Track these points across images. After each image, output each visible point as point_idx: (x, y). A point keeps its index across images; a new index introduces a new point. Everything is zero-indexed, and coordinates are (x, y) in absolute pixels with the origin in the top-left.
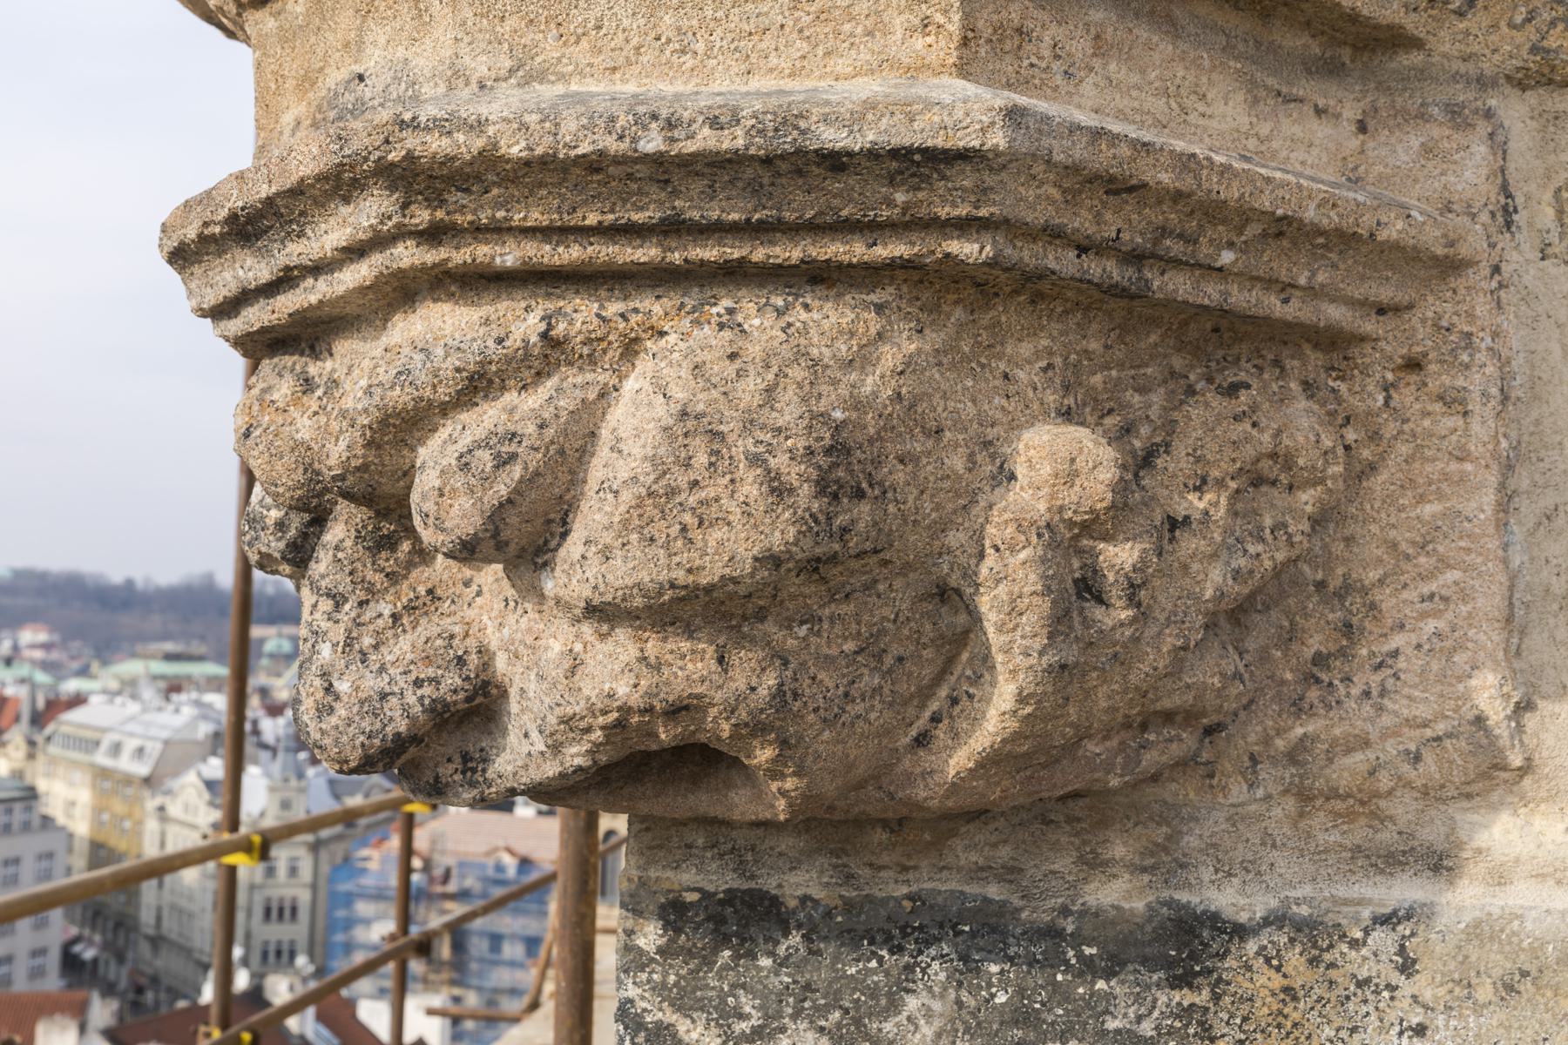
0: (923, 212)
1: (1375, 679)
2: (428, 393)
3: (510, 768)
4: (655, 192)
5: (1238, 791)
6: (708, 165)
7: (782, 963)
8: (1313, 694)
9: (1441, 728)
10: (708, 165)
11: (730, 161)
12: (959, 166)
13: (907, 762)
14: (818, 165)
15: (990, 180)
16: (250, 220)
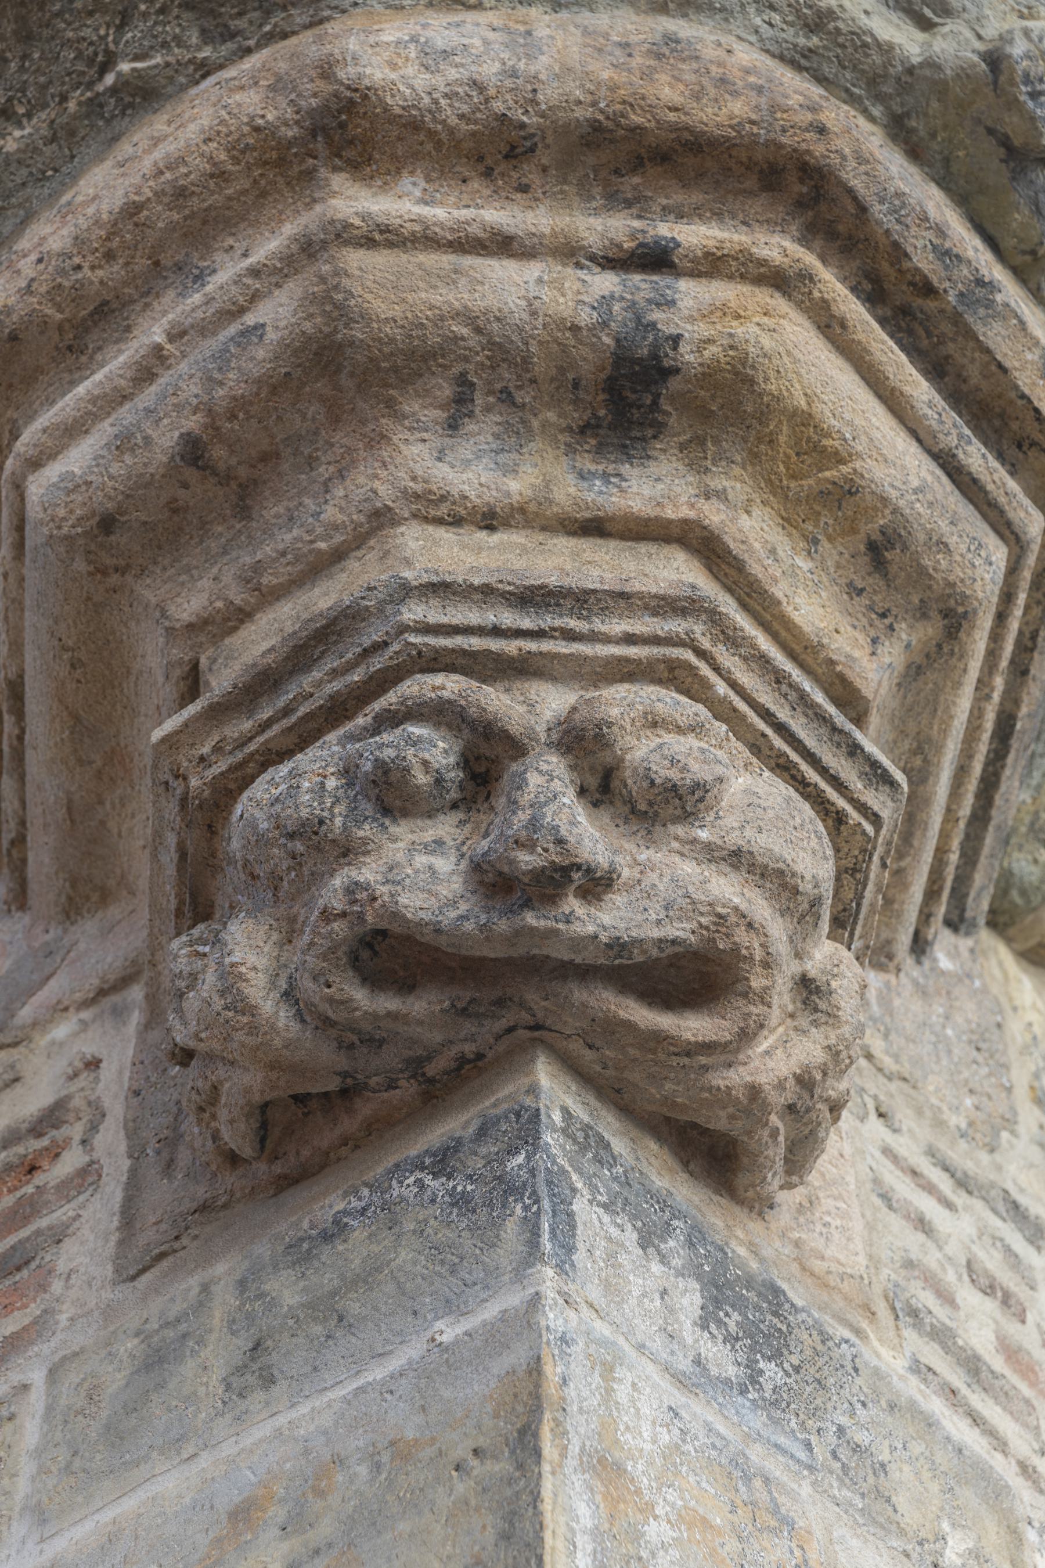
0: (863, 799)
1: (824, 1230)
2: (678, 716)
3: (623, 925)
4: (787, 708)
5: (778, 1244)
6: (816, 714)
7: (615, 1179)
8: (802, 1220)
9: (849, 1271)
10: (816, 714)
11: (824, 718)
12: (887, 788)
13: (756, 1063)
14: (848, 746)
15: (890, 803)
16: (551, 593)
